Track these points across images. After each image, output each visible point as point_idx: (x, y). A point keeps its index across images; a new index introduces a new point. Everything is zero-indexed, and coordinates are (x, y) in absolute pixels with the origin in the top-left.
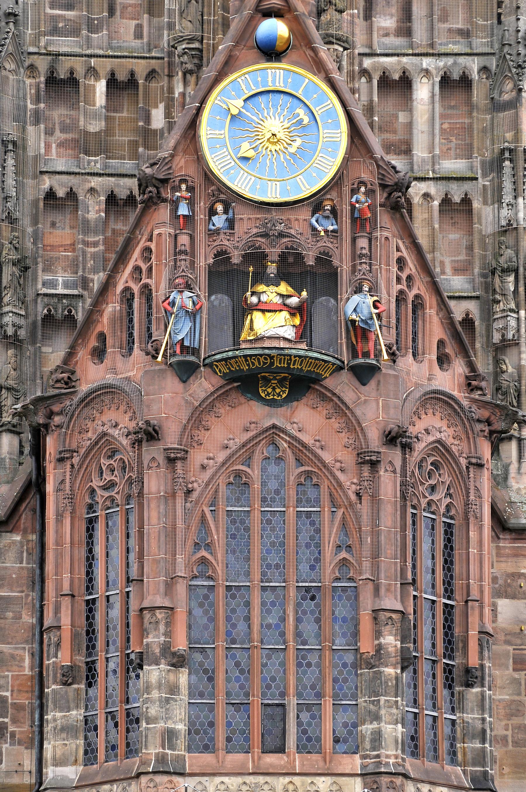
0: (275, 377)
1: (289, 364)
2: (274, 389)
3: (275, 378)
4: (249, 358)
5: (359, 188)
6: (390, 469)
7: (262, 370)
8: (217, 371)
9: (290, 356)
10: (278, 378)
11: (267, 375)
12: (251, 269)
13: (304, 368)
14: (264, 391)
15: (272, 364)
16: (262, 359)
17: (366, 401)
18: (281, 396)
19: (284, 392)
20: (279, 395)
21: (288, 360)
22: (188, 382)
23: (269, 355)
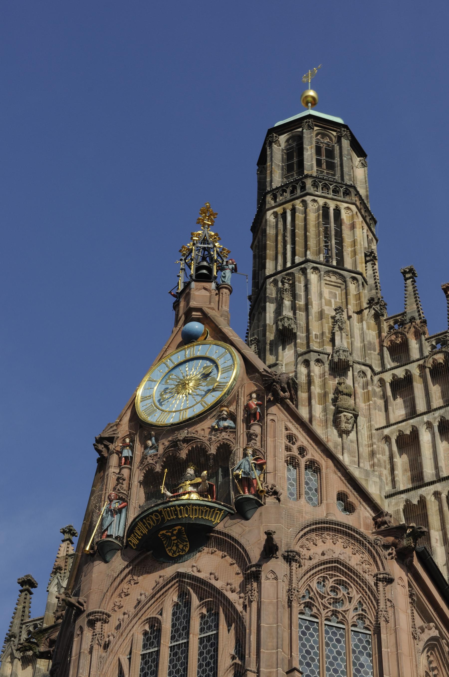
0: (172, 533)
1: (177, 515)
2: (177, 546)
3: (173, 535)
4: (144, 520)
5: (251, 397)
6: (270, 576)
7: (158, 529)
8: (132, 545)
9: (174, 506)
10: (175, 532)
11: (164, 532)
12: (166, 470)
13: (191, 517)
14: (170, 550)
15: (163, 519)
16: (154, 517)
17: (249, 531)
18: (185, 551)
19: (186, 546)
20: (183, 550)
21: (174, 511)
22: (111, 562)
23: (157, 511)
